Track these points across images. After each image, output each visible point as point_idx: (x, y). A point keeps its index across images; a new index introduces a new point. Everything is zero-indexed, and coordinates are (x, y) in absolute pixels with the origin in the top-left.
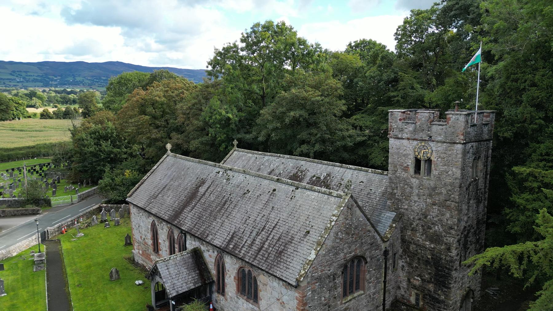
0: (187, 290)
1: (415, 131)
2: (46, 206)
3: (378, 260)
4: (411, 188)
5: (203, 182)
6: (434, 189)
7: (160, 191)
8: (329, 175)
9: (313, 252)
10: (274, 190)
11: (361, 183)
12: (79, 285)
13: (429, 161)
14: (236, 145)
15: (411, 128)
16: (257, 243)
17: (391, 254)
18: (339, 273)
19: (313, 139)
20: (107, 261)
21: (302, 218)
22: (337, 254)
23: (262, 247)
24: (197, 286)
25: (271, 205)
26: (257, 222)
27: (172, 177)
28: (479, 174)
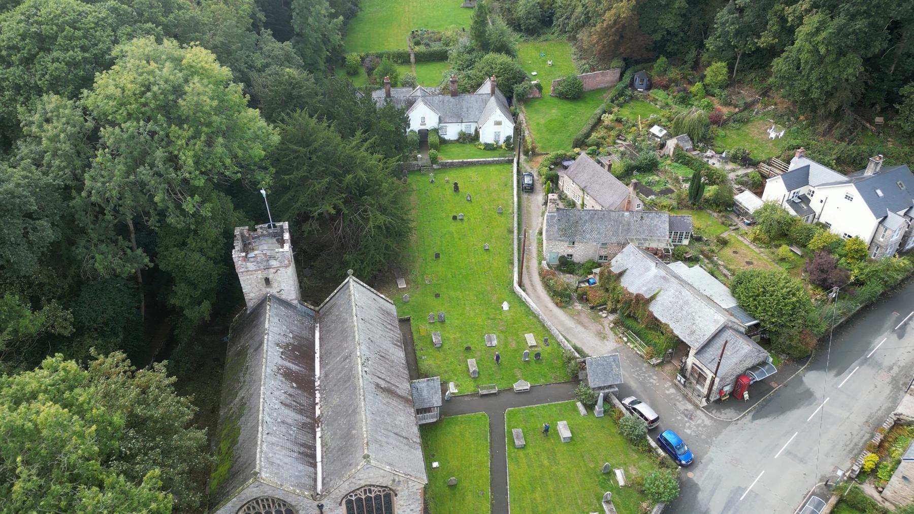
5: (378, 386)
7: (401, 439)
8: (278, 345)
27: (386, 432)
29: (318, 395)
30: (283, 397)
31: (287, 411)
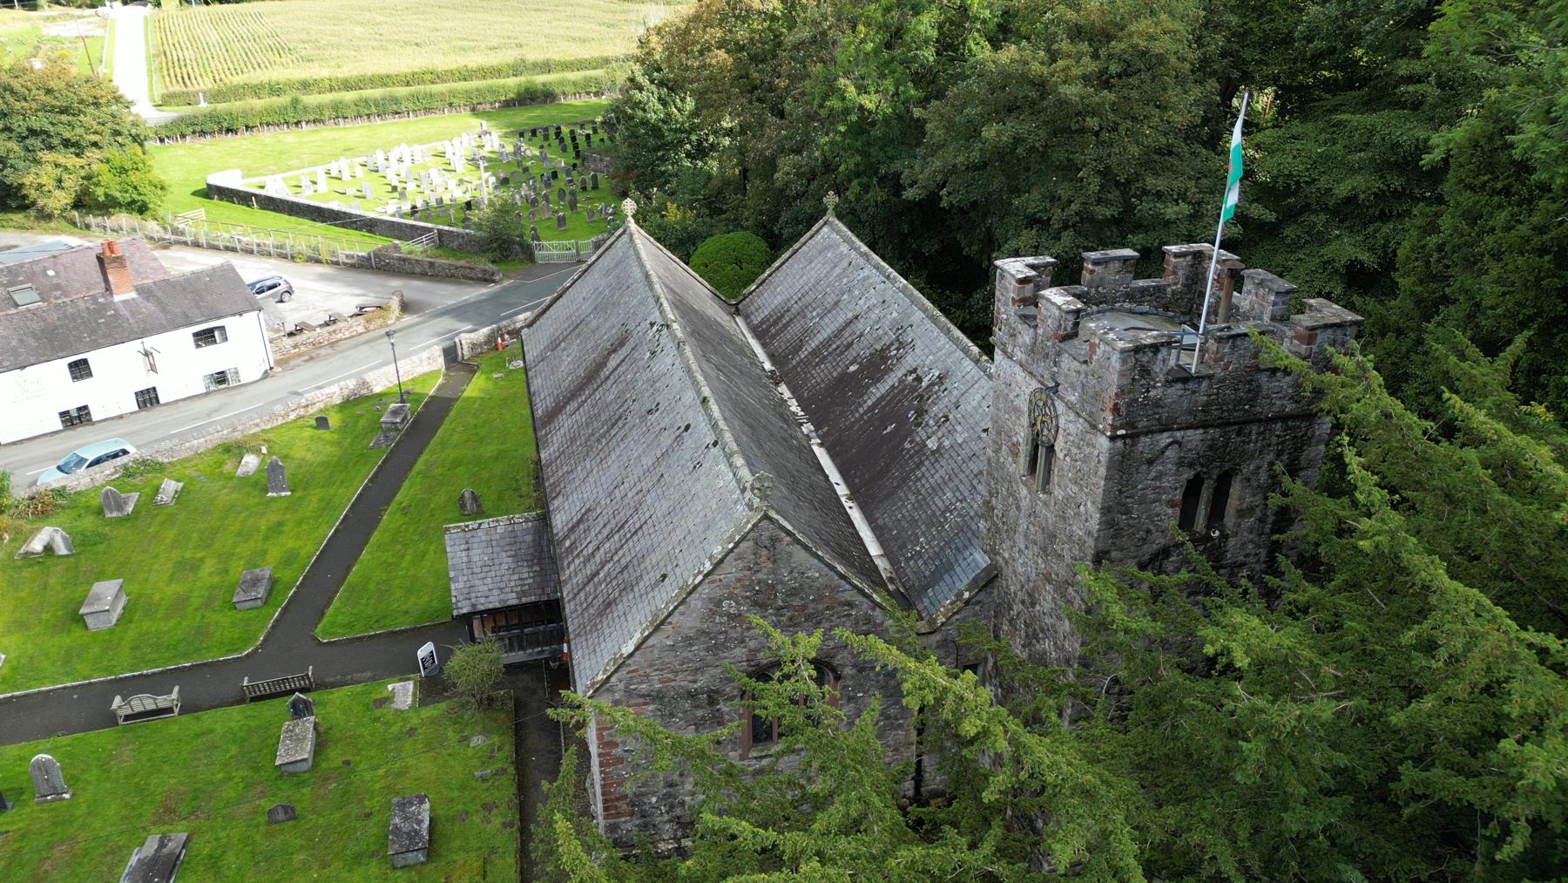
0: (498, 605)
1: (1032, 350)
2: (522, 261)
4: (1018, 508)
5: (622, 344)
6: (1052, 537)
9: (637, 637)
10: (687, 427)
11: (984, 435)
12: (405, 510)
13: (1051, 449)
14: (831, 207)
15: (1026, 337)
16: (597, 558)
19: (1057, 215)
20: (496, 458)
21: (678, 531)
22: (715, 649)
23: (597, 573)
24: (524, 600)
25: (662, 469)
26: (626, 501)
28: (1230, 519)
29: (794, 407)
30: (860, 326)
31: (841, 320)
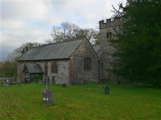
3: (96, 63)
17: (100, 63)
18: (83, 60)
